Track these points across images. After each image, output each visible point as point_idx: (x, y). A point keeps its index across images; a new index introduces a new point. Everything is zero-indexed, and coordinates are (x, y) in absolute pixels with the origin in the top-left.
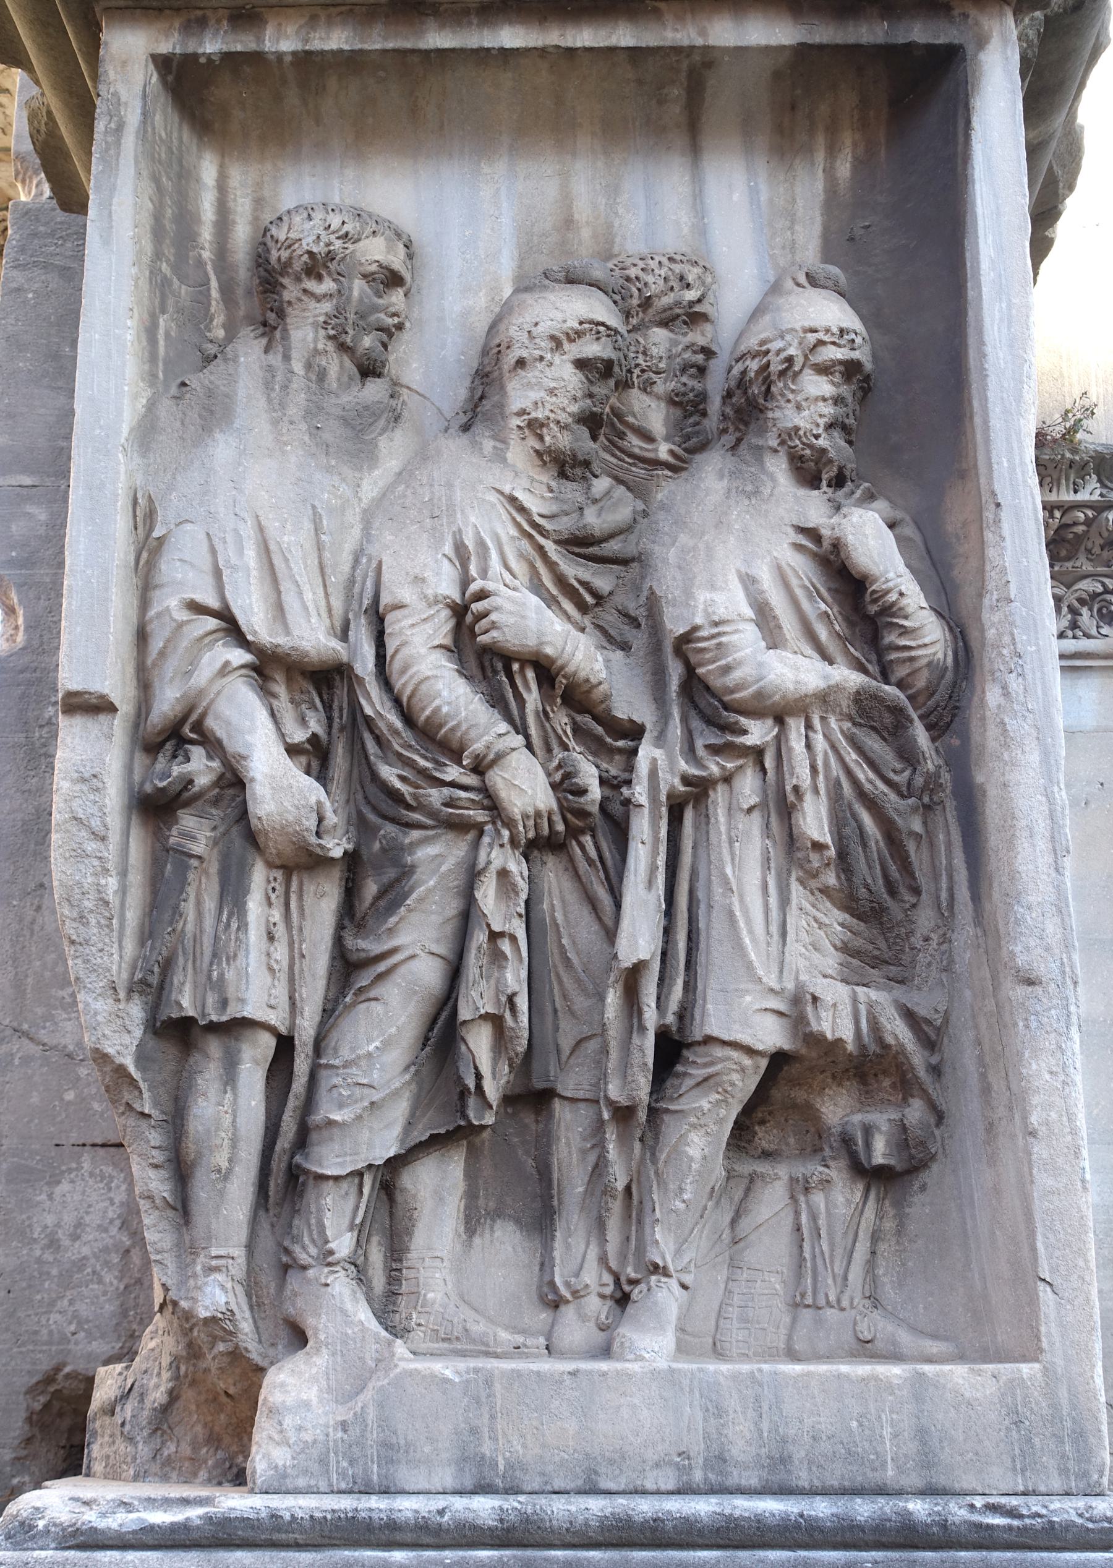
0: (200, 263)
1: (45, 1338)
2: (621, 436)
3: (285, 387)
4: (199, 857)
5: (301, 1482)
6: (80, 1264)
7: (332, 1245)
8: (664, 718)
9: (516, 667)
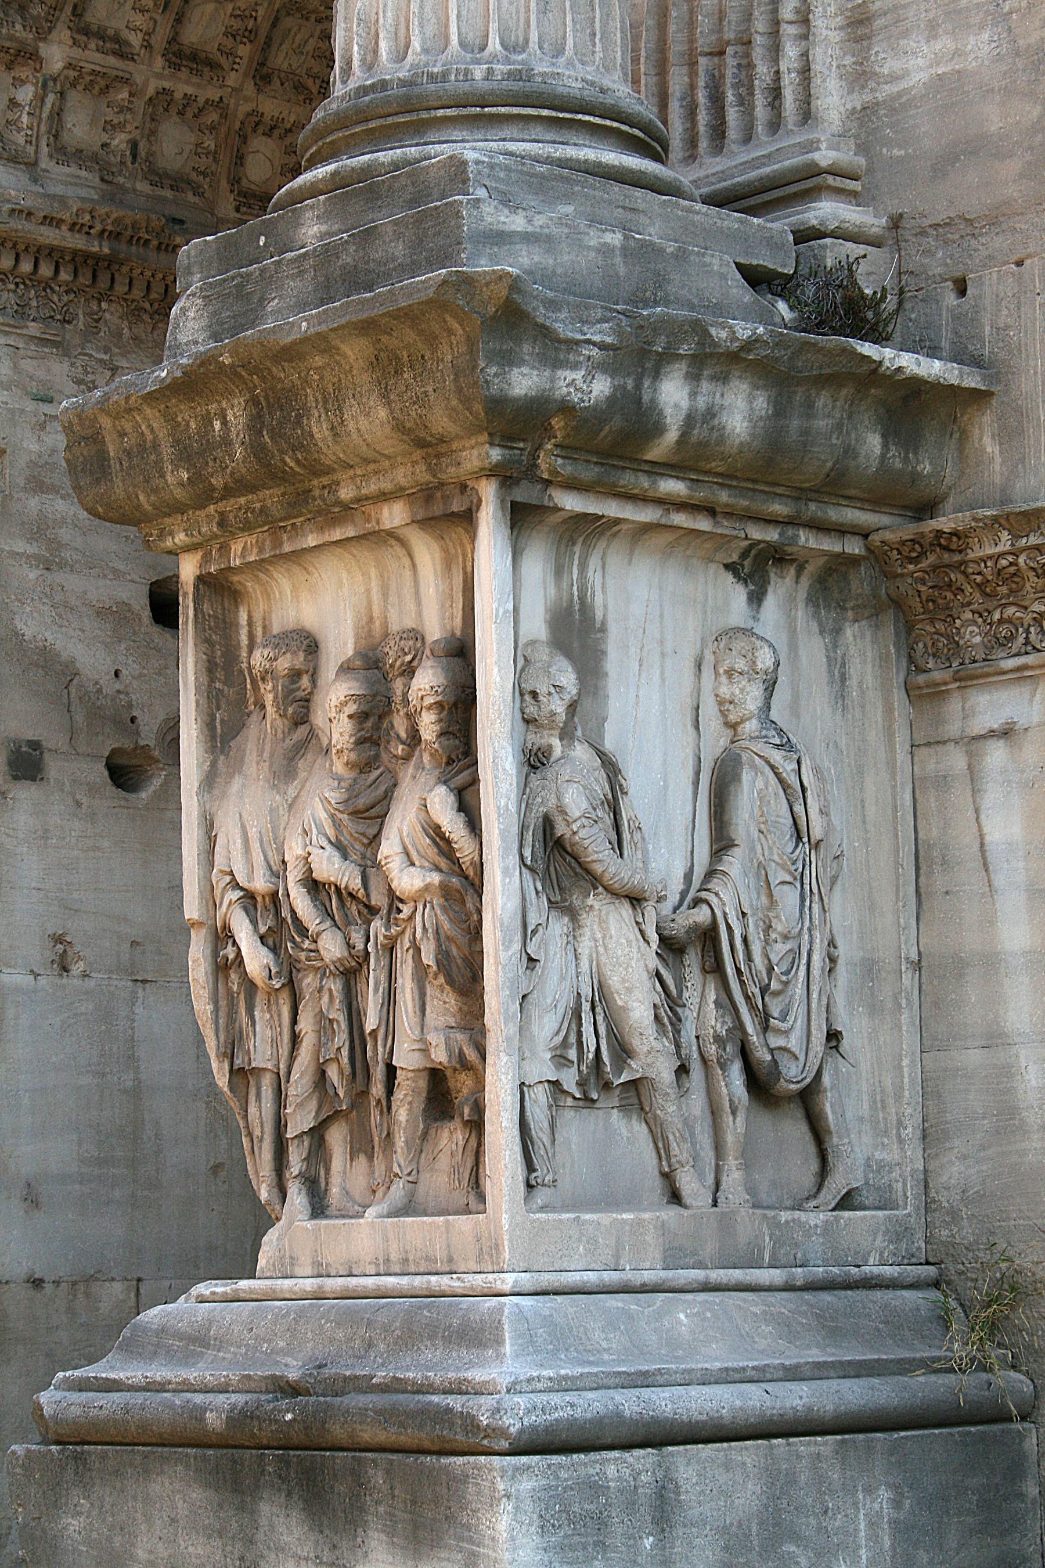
5: (268, 1274)
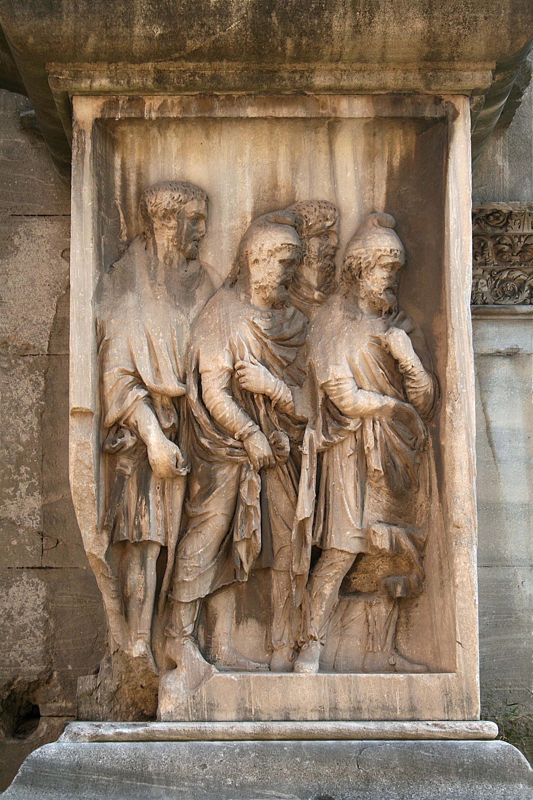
0: (116, 206)
1: (8, 663)
2: (299, 287)
3: (155, 267)
4: (129, 475)
5: (178, 718)
6: (24, 627)
7: (186, 629)
8: (316, 415)
9: (255, 397)
